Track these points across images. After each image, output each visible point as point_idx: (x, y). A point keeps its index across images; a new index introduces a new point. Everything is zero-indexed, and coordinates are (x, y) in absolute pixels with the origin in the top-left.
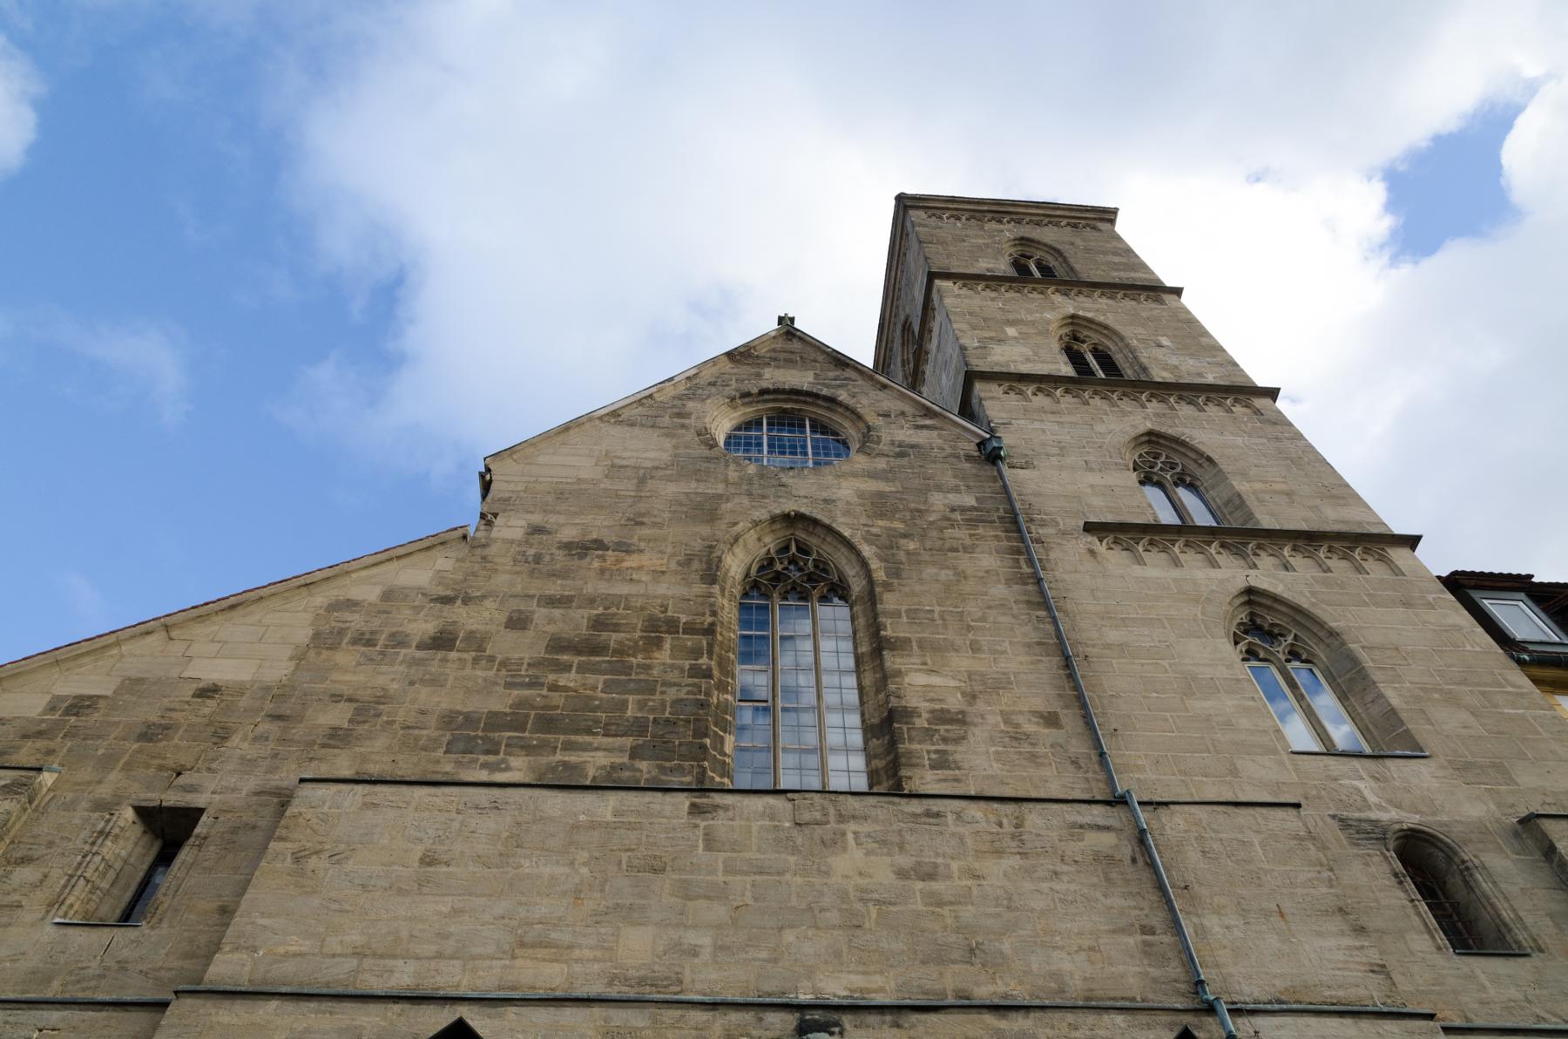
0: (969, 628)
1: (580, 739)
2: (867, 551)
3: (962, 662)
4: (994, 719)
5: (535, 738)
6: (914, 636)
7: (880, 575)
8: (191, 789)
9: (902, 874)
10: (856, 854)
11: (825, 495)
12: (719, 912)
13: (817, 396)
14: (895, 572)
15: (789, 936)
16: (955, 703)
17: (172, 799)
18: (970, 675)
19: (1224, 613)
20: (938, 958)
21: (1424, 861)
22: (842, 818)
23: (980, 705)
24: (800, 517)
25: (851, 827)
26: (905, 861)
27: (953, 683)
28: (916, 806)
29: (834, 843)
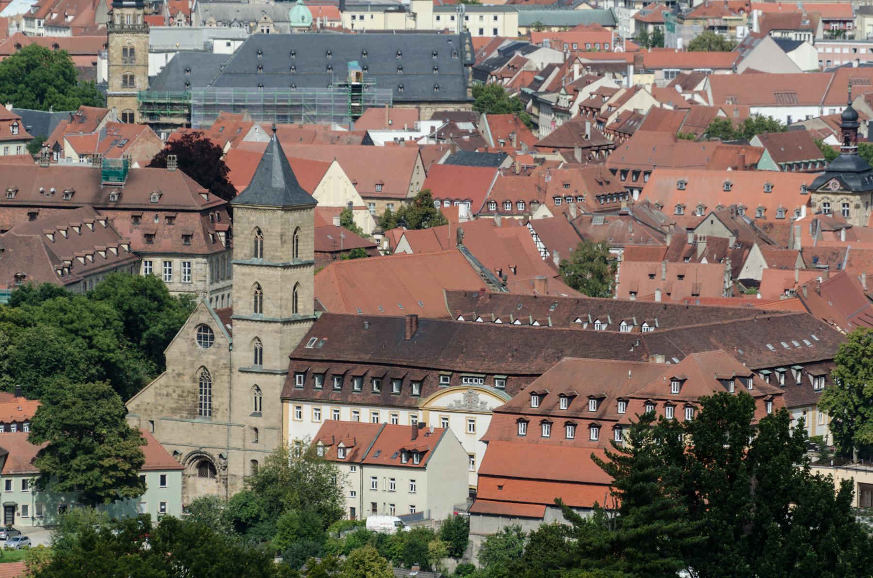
3: (220, 400)
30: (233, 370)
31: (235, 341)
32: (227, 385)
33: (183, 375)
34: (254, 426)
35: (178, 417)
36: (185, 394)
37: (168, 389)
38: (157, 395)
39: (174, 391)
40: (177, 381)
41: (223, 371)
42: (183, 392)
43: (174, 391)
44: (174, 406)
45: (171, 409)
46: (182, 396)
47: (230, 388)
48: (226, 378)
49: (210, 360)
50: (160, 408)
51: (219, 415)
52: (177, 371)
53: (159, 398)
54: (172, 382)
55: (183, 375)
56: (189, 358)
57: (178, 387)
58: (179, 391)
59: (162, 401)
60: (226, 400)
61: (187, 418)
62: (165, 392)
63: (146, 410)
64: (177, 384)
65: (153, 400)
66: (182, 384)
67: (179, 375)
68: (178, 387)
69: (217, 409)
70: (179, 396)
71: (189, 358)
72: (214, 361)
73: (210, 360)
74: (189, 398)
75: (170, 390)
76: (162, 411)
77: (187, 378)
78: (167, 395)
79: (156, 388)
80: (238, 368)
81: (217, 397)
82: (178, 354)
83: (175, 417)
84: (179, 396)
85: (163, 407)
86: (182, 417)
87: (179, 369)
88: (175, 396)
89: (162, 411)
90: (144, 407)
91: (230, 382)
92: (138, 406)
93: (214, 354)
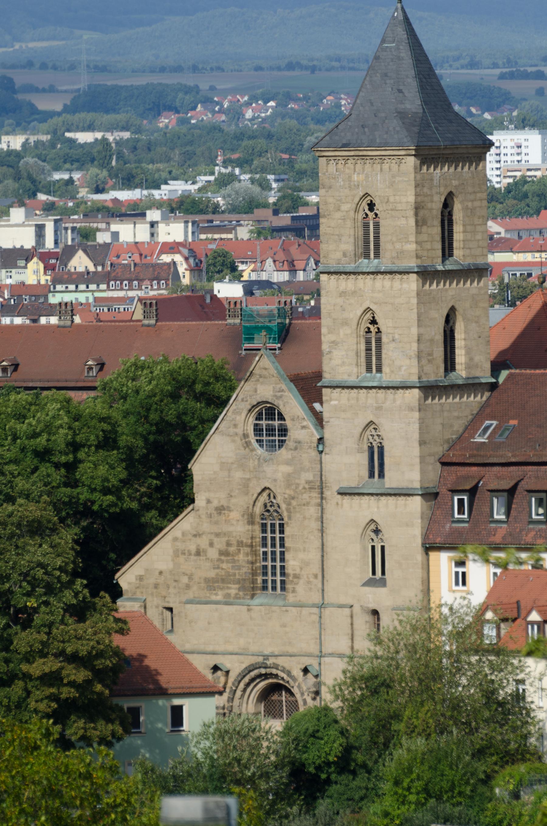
0: (304, 542)
3: (301, 555)
4: (305, 577)
30: (327, 493)
32: (315, 525)
33: (229, 509)
36: (232, 549)
37: (198, 541)
39: (211, 545)
40: (216, 523)
41: (306, 496)
42: (228, 544)
43: (211, 545)
45: (207, 580)
48: (312, 511)
49: (279, 476)
51: (301, 588)
54: (206, 527)
55: (229, 509)
56: (238, 475)
57: (217, 535)
58: (220, 543)
60: (314, 556)
61: (237, 597)
64: (216, 529)
66: (226, 528)
67: (220, 510)
68: (217, 535)
69: (296, 576)
70: (221, 553)
71: (238, 475)
72: (288, 478)
73: (279, 476)
75: (203, 542)
76: (188, 587)
77: (235, 515)
83: (214, 598)
84: (221, 553)
85: (190, 577)
86: (228, 595)
87: (219, 498)
88: (213, 553)
89: (188, 587)
93: (288, 463)
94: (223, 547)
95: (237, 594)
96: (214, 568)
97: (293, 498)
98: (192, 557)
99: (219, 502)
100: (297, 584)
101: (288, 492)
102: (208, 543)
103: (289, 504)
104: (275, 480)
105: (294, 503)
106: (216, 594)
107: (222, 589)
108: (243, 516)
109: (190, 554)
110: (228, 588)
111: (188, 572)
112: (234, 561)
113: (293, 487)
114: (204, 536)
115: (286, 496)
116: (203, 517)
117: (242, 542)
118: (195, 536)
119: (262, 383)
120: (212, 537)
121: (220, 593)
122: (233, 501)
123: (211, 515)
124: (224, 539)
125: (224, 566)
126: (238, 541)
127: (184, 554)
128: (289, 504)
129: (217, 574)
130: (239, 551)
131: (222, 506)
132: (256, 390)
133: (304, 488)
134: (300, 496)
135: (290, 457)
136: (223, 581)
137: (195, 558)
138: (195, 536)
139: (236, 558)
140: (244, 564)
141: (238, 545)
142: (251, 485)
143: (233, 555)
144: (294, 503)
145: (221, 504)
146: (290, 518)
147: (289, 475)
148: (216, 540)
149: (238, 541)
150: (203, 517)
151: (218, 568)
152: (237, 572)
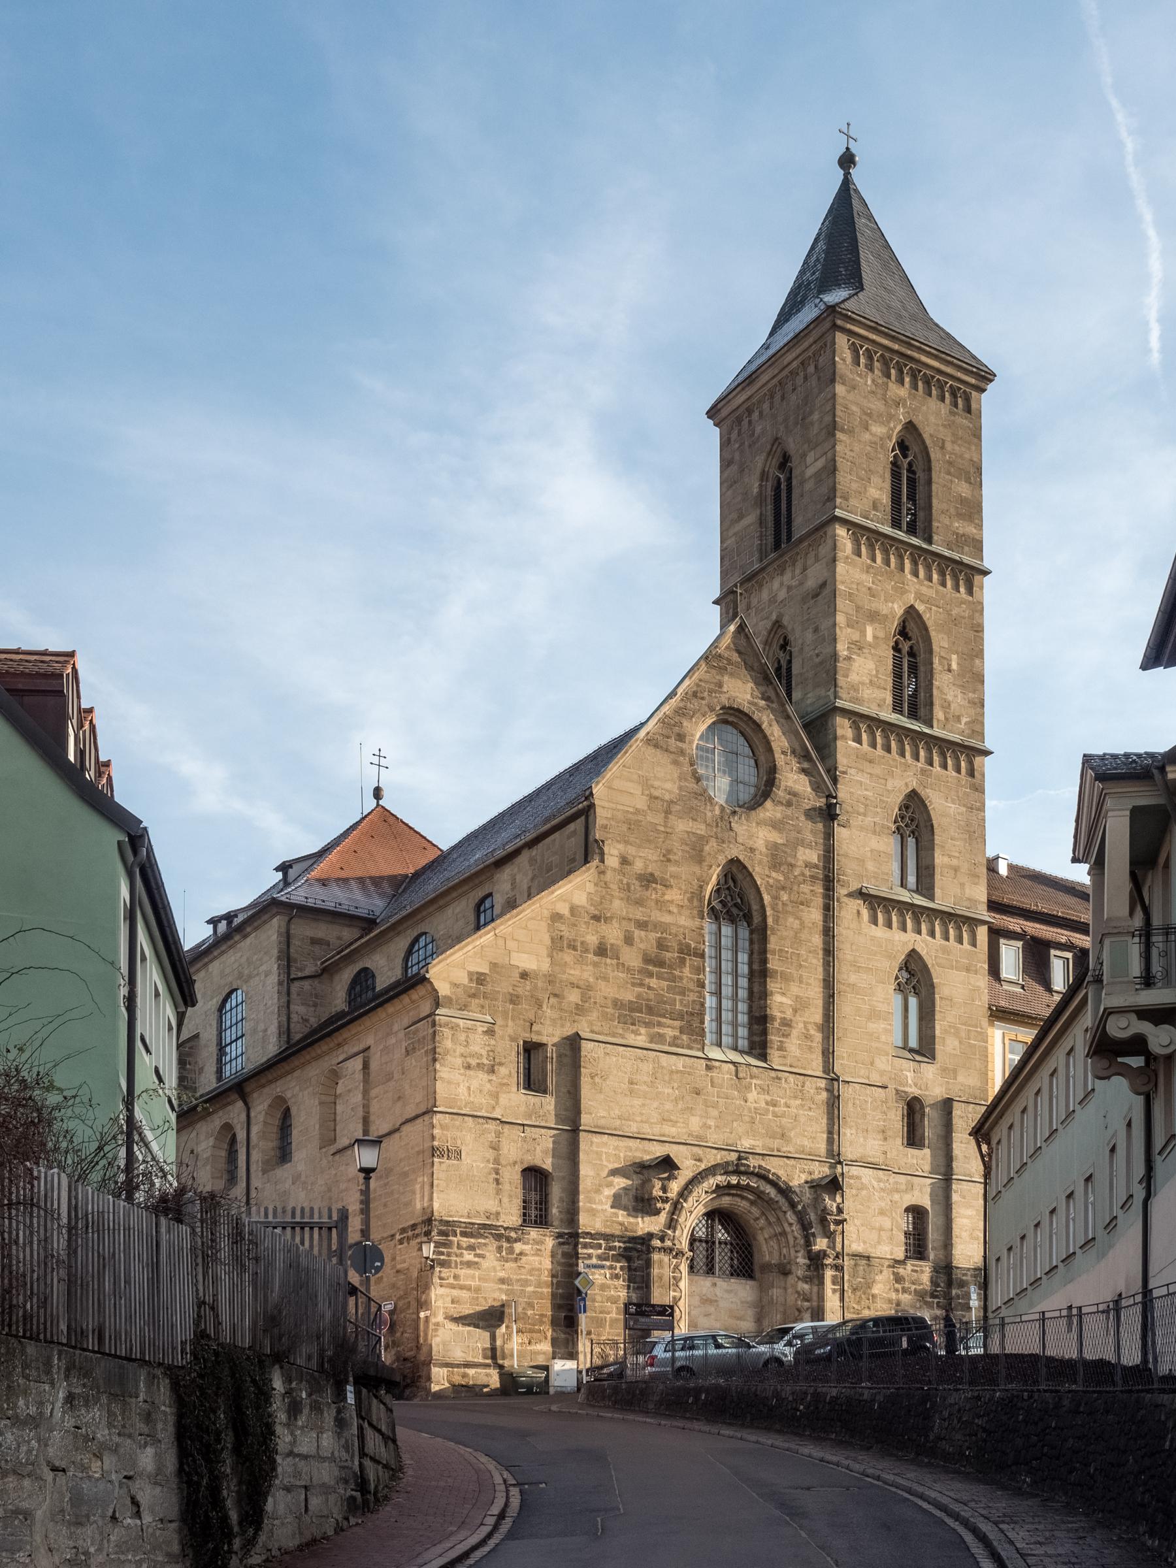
1: (664, 1020)
2: (767, 898)
3: (795, 989)
4: (801, 1025)
5: (647, 1018)
6: (780, 969)
7: (770, 921)
8: (539, 1033)
9: (767, 1103)
10: (755, 1093)
11: (750, 843)
12: (715, 1113)
13: (750, 718)
14: (776, 920)
15: (735, 1124)
16: (789, 1014)
17: (535, 1038)
18: (797, 997)
19: (891, 967)
20: (773, 1137)
21: (913, 1109)
22: (752, 1077)
23: (798, 1018)
24: (738, 861)
25: (754, 1081)
26: (768, 1098)
27: (790, 1002)
28: (773, 1074)
29: (748, 1088)
31: (843, 792)
32: (817, 940)
34: (913, 1091)
35: (641, 1040)
38: (558, 944)
40: (639, 903)
41: (805, 888)
42: (661, 945)
43: (629, 940)
44: (628, 996)
45: (616, 1003)
46: (661, 963)
47: (829, 952)
48: (815, 915)
49: (760, 844)
50: (573, 997)
51: (793, 1045)
52: (638, 866)
53: (568, 957)
57: (642, 925)
58: (646, 941)
59: (582, 972)
60: (815, 993)
62: (592, 939)
63: (514, 999)
64: (639, 914)
65: (545, 966)
67: (648, 880)
68: (642, 925)
69: (786, 1023)
71: (682, 826)
72: (774, 848)
73: (760, 844)
74: (687, 971)
75: (613, 933)
76: (580, 1010)
77: (673, 895)
78: (601, 951)
79: (556, 917)
80: (854, 886)
81: (787, 978)
82: (641, 803)
83: (631, 1039)
84: (647, 960)
86: (660, 1038)
87: (645, 859)
88: (631, 957)
89: (580, 1010)
90: (504, 987)
91: (828, 933)
92: (480, 979)
93: (776, 825)
94: (653, 950)
95: (675, 1038)
96: (633, 985)
97: (783, 888)
98: (591, 956)
99: (646, 866)
100: (787, 1036)
101: (774, 874)
102: (621, 936)
103: (776, 898)
104: (752, 850)
105: (785, 897)
106: (637, 1033)
107: (647, 1025)
108: (690, 900)
109: (587, 951)
110: (660, 1024)
111: (581, 983)
112: (673, 979)
113: (784, 868)
114: (615, 923)
115: (771, 881)
116: (614, 887)
117: (688, 946)
118: (597, 918)
119: (732, 675)
120: (631, 927)
121: (643, 1030)
122: (672, 869)
123: (628, 884)
124: (654, 936)
125: (653, 983)
126: (680, 944)
127: (575, 949)
128: (776, 898)
129: (639, 996)
130: (682, 962)
131: (652, 875)
132: (720, 685)
133: (803, 874)
134: (795, 888)
135: (779, 815)
136: (650, 1010)
137: (596, 959)
138: (597, 918)
139: (677, 973)
140: (691, 986)
141: (681, 951)
142: (707, 848)
143: (670, 967)
144: (785, 897)
145: (650, 870)
146: (776, 920)
147: (775, 846)
148: (637, 933)
149: (680, 944)
150: (614, 887)
151: (641, 985)
152: (678, 997)
